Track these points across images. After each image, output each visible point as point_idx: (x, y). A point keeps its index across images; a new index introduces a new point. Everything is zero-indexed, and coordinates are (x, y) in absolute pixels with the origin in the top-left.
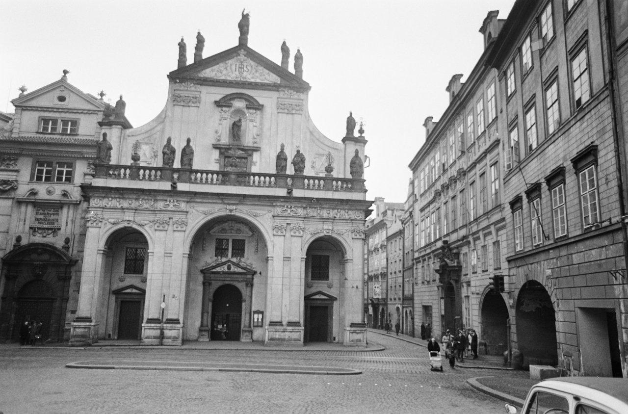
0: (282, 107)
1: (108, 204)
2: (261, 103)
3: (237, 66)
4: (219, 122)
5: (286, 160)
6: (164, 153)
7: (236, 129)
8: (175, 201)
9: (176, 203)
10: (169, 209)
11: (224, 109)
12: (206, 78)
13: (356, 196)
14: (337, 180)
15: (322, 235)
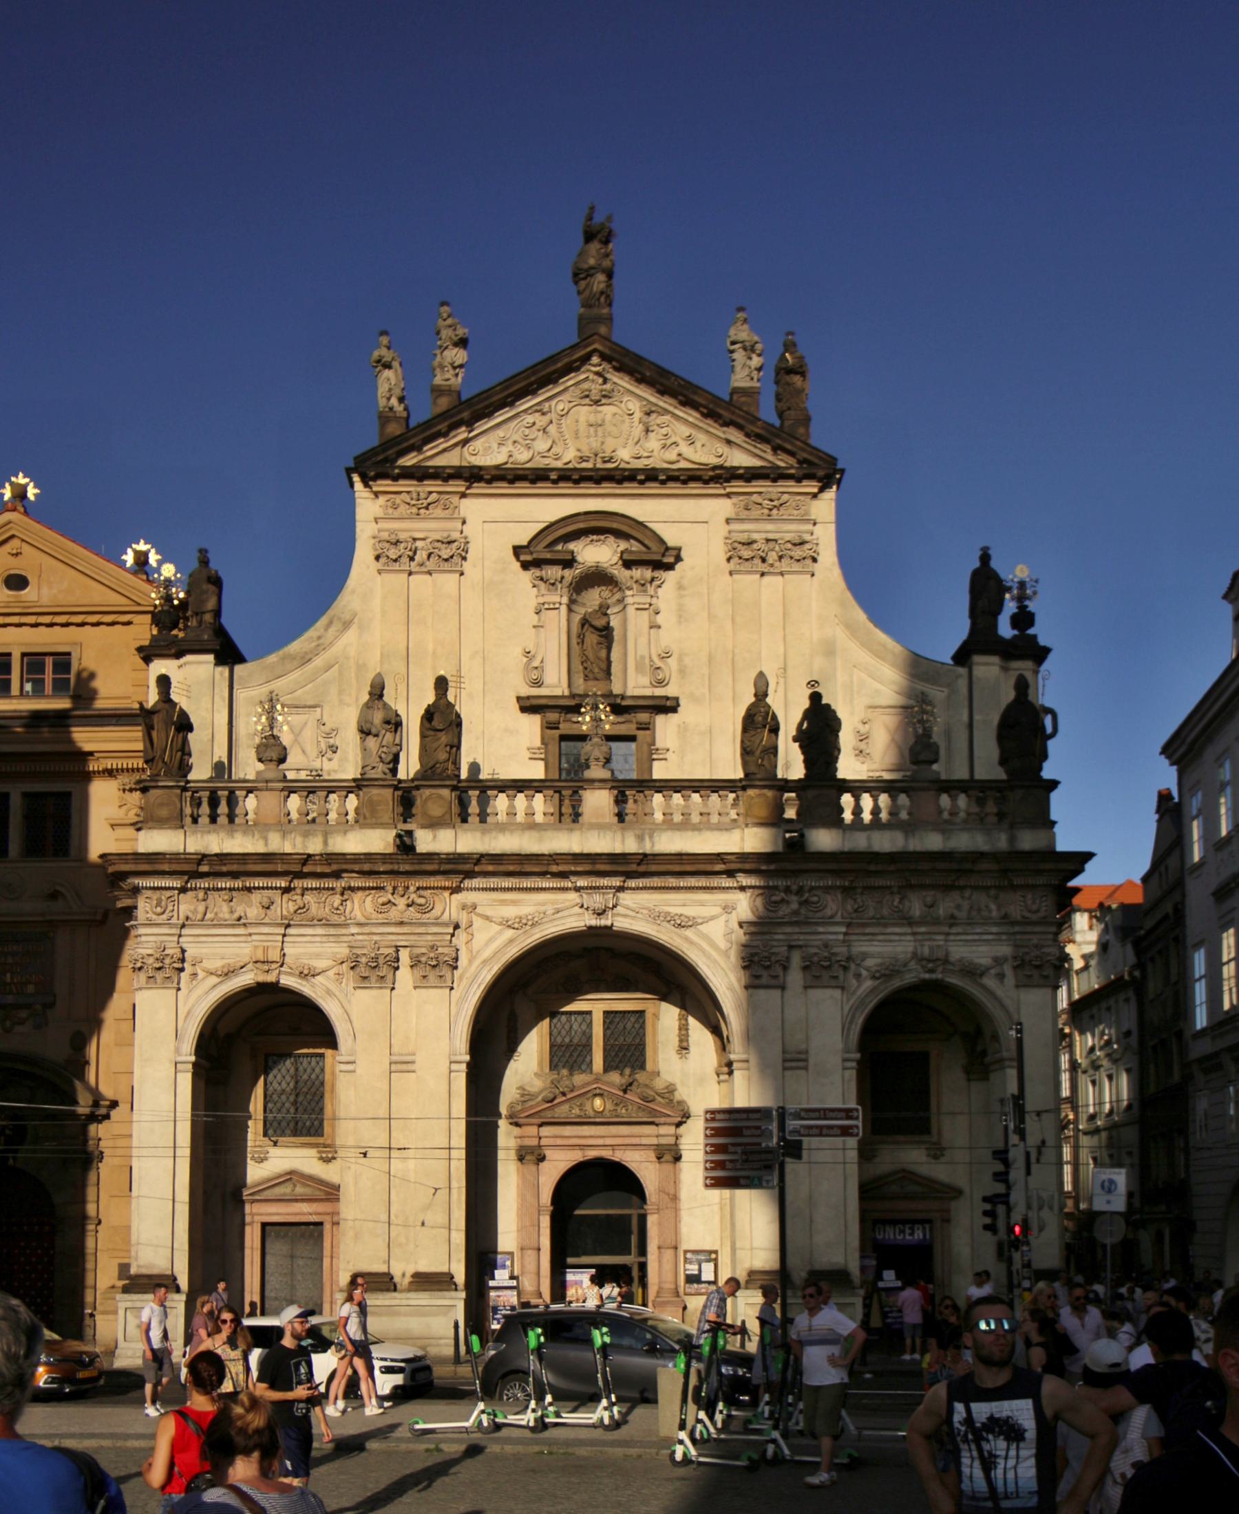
0: (746, 553)
1: (195, 911)
2: (671, 543)
3: (582, 419)
4: (534, 619)
5: (775, 730)
6: (365, 732)
7: (595, 639)
8: (412, 889)
9: (413, 896)
10: (394, 914)
11: (553, 572)
12: (480, 468)
13: (1028, 841)
14: (950, 787)
15: (909, 978)
